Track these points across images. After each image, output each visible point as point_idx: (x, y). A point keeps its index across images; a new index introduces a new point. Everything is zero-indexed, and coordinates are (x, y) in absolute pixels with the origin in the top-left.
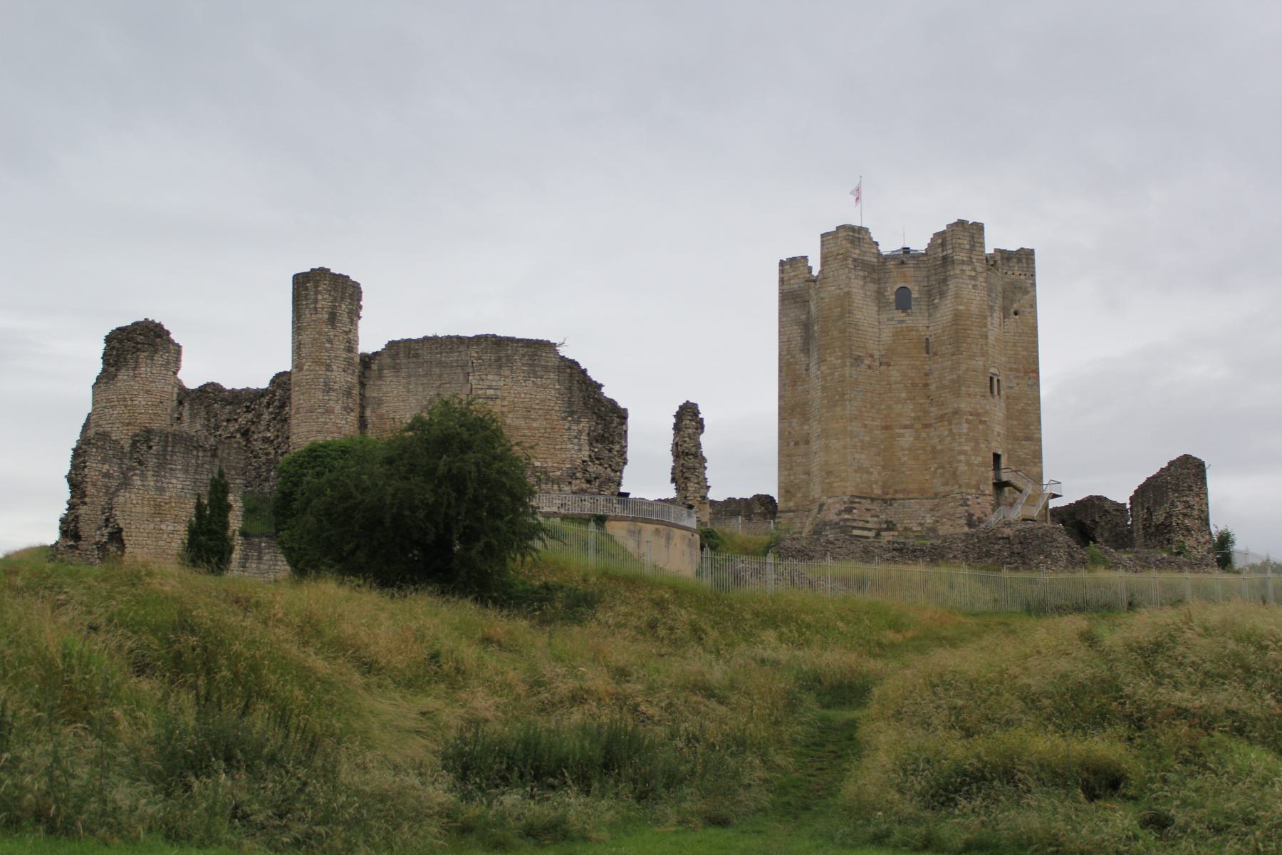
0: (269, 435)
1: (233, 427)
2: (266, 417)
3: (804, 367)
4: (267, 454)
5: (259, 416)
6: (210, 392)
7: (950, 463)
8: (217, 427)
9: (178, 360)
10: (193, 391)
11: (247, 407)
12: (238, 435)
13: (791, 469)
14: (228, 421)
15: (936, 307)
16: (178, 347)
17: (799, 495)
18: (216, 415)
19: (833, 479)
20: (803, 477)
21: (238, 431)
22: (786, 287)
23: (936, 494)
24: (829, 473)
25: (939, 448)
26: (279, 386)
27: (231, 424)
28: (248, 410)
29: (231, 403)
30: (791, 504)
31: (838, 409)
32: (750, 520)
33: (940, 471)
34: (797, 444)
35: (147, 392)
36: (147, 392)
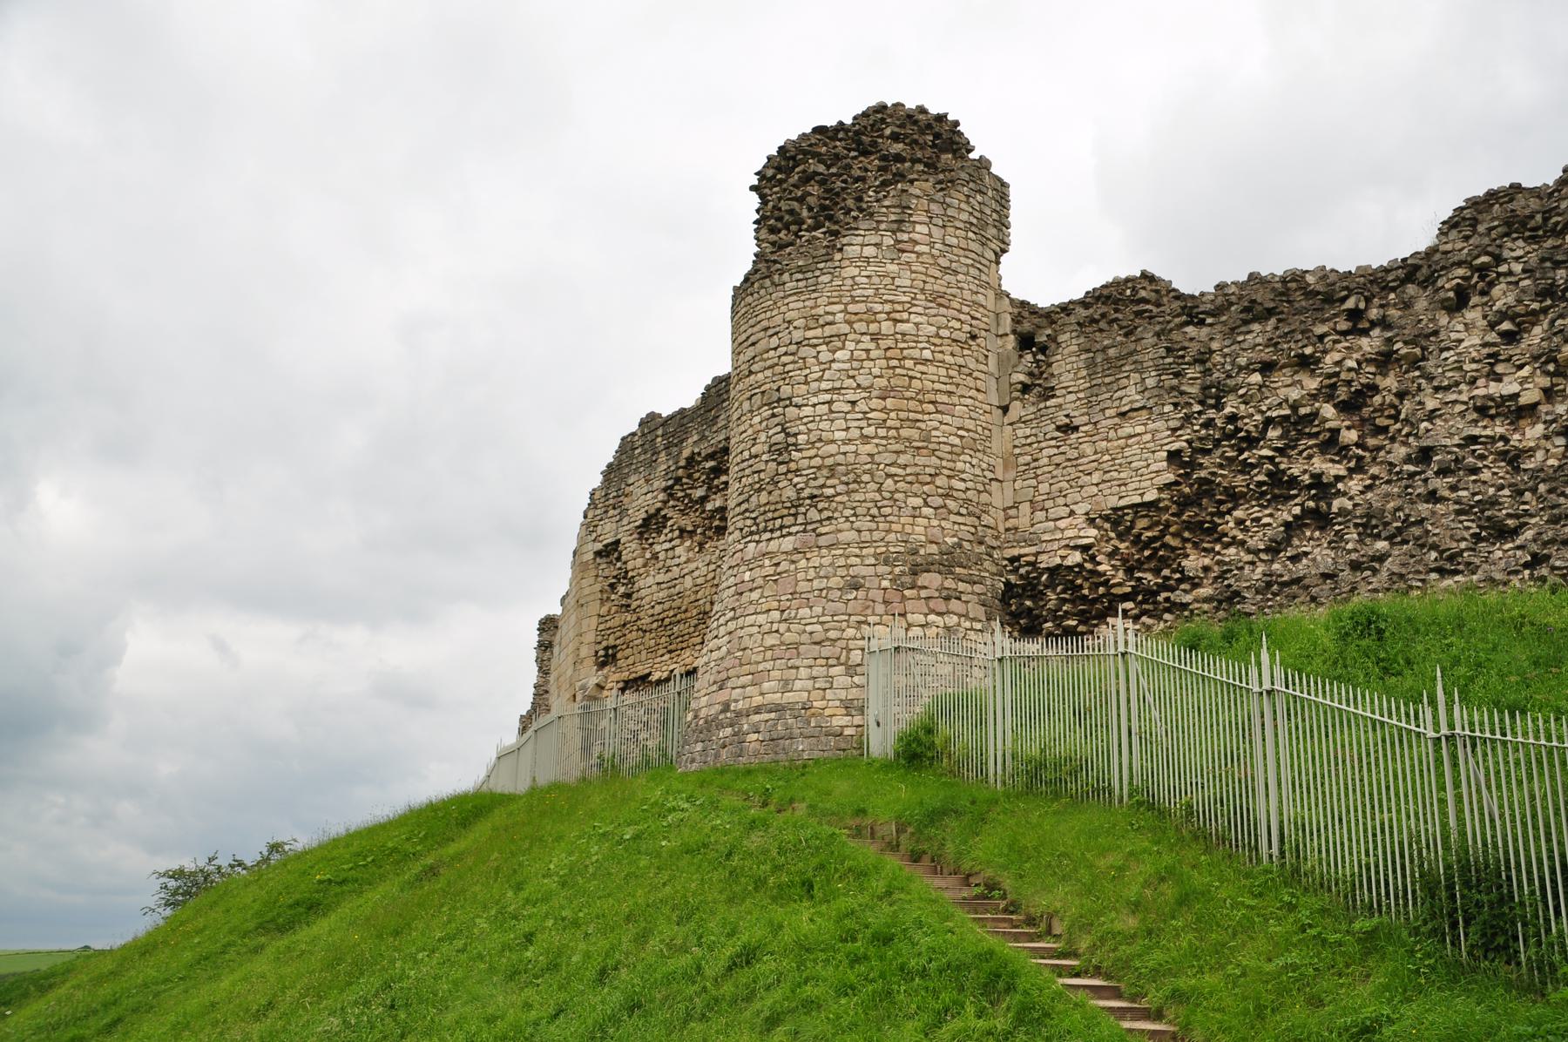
0: (1509, 387)
1: (1293, 388)
2: (1468, 334)
4: (1513, 459)
5: (1425, 338)
6: (1129, 306)
8: (1214, 395)
9: (1003, 224)
10: (1065, 309)
11: (1355, 315)
12: (1328, 410)
14: (1267, 368)
16: (1004, 185)
18: (1202, 359)
21: (1328, 393)
26: (1516, 226)
27: (1281, 378)
28: (1358, 323)
29: (1270, 312)
35: (937, 299)
36: (937, 299)
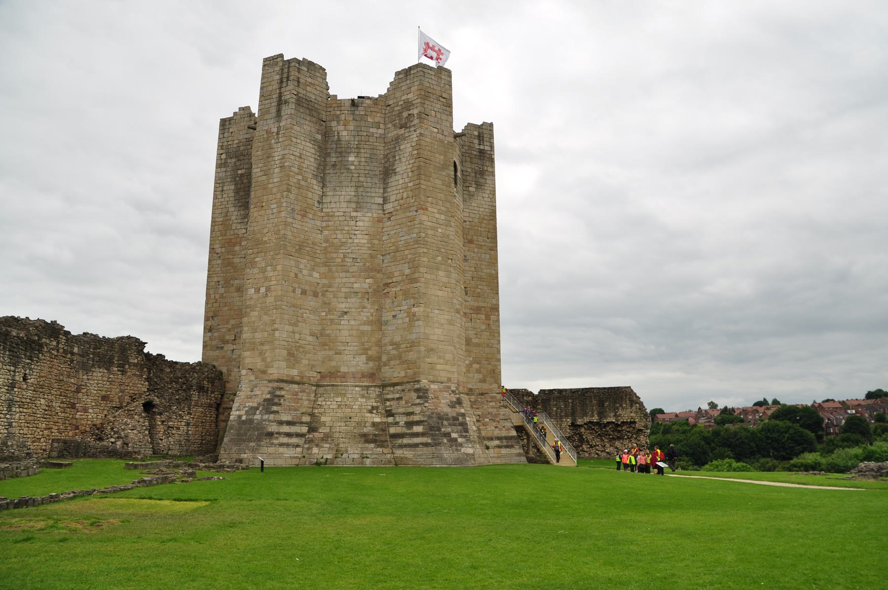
3: (316, 198)
7: (487, 359)
13: (295, 325)
15: (471, 195)
17: (305, 362)
19: (433, 359)
20: (311, 339)
22: (301, 91)
23: (471, 390)
24: (430, 350)
25: (475, 341)
30: (294, 372)
31: (441, 273)
32: (124, 372)
33: (476, 366)
34: (304, 292)
